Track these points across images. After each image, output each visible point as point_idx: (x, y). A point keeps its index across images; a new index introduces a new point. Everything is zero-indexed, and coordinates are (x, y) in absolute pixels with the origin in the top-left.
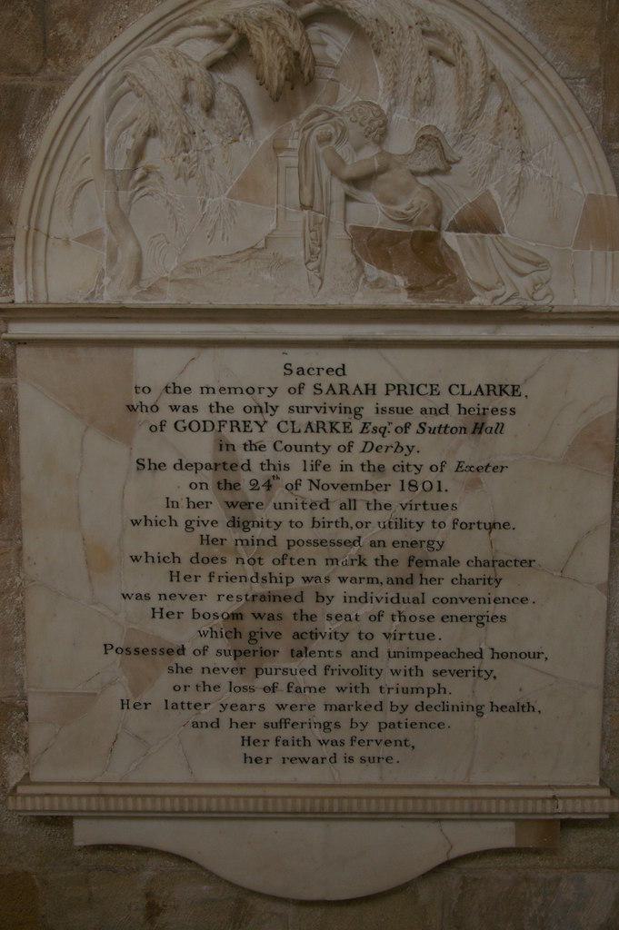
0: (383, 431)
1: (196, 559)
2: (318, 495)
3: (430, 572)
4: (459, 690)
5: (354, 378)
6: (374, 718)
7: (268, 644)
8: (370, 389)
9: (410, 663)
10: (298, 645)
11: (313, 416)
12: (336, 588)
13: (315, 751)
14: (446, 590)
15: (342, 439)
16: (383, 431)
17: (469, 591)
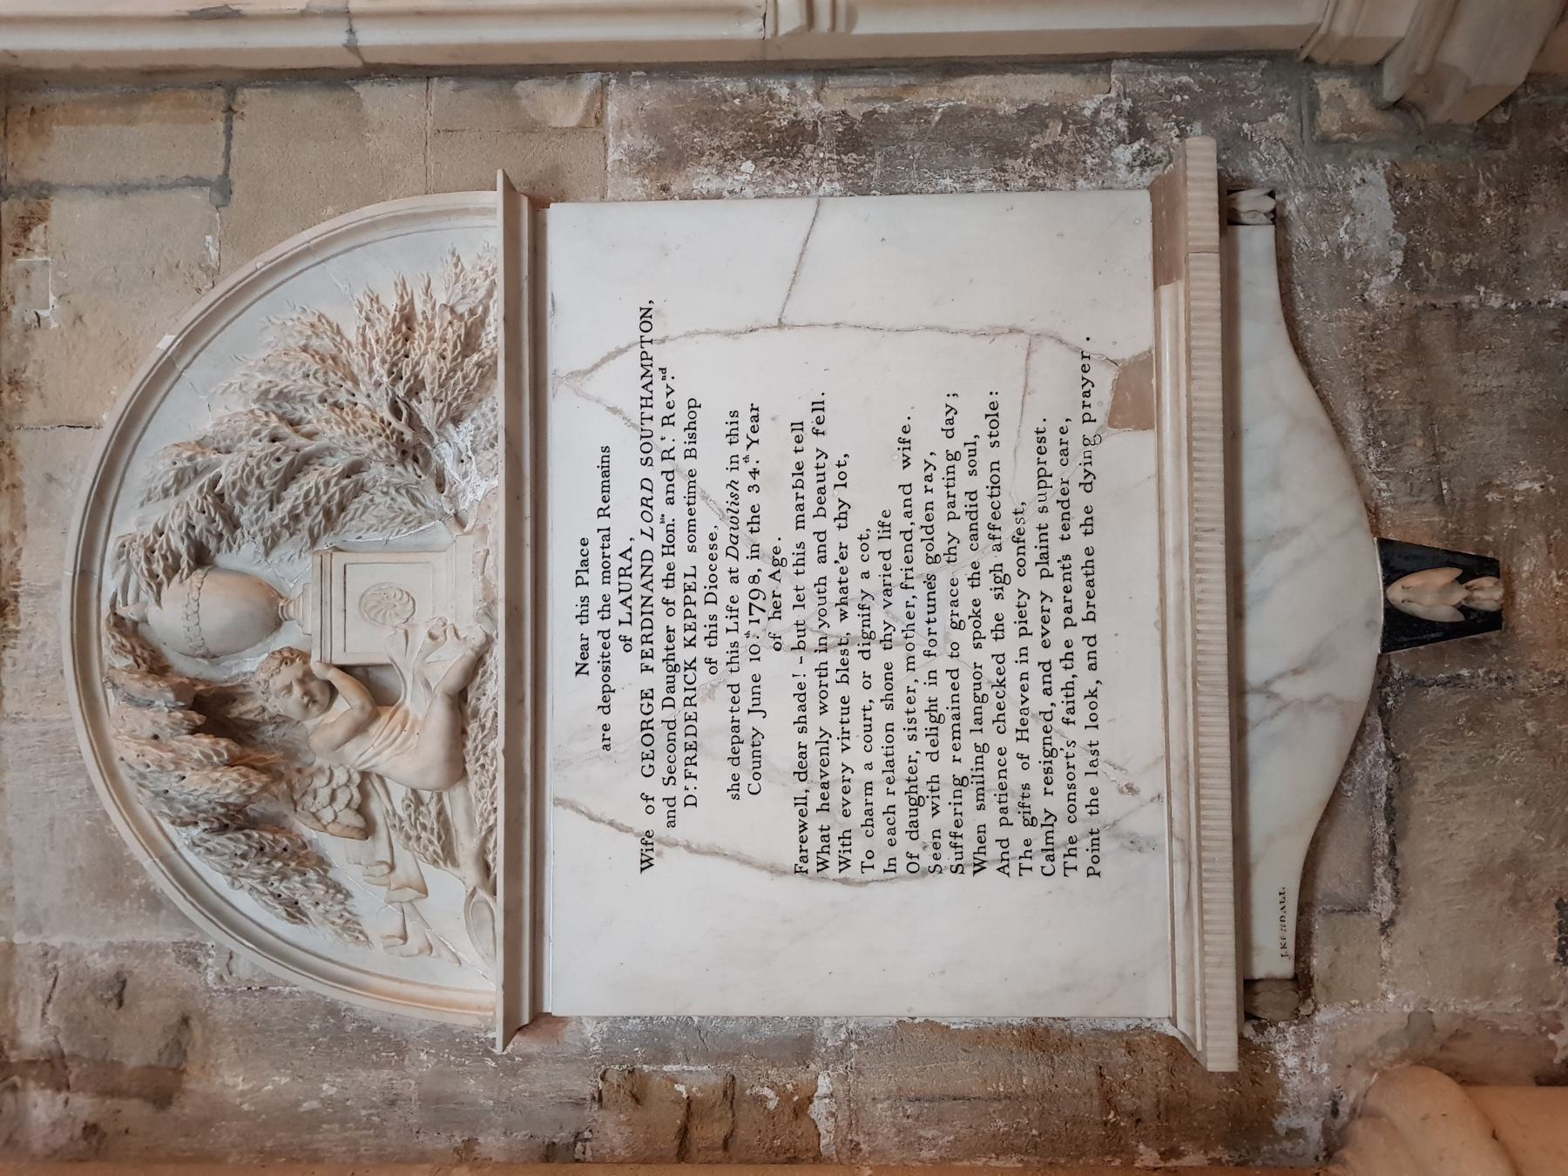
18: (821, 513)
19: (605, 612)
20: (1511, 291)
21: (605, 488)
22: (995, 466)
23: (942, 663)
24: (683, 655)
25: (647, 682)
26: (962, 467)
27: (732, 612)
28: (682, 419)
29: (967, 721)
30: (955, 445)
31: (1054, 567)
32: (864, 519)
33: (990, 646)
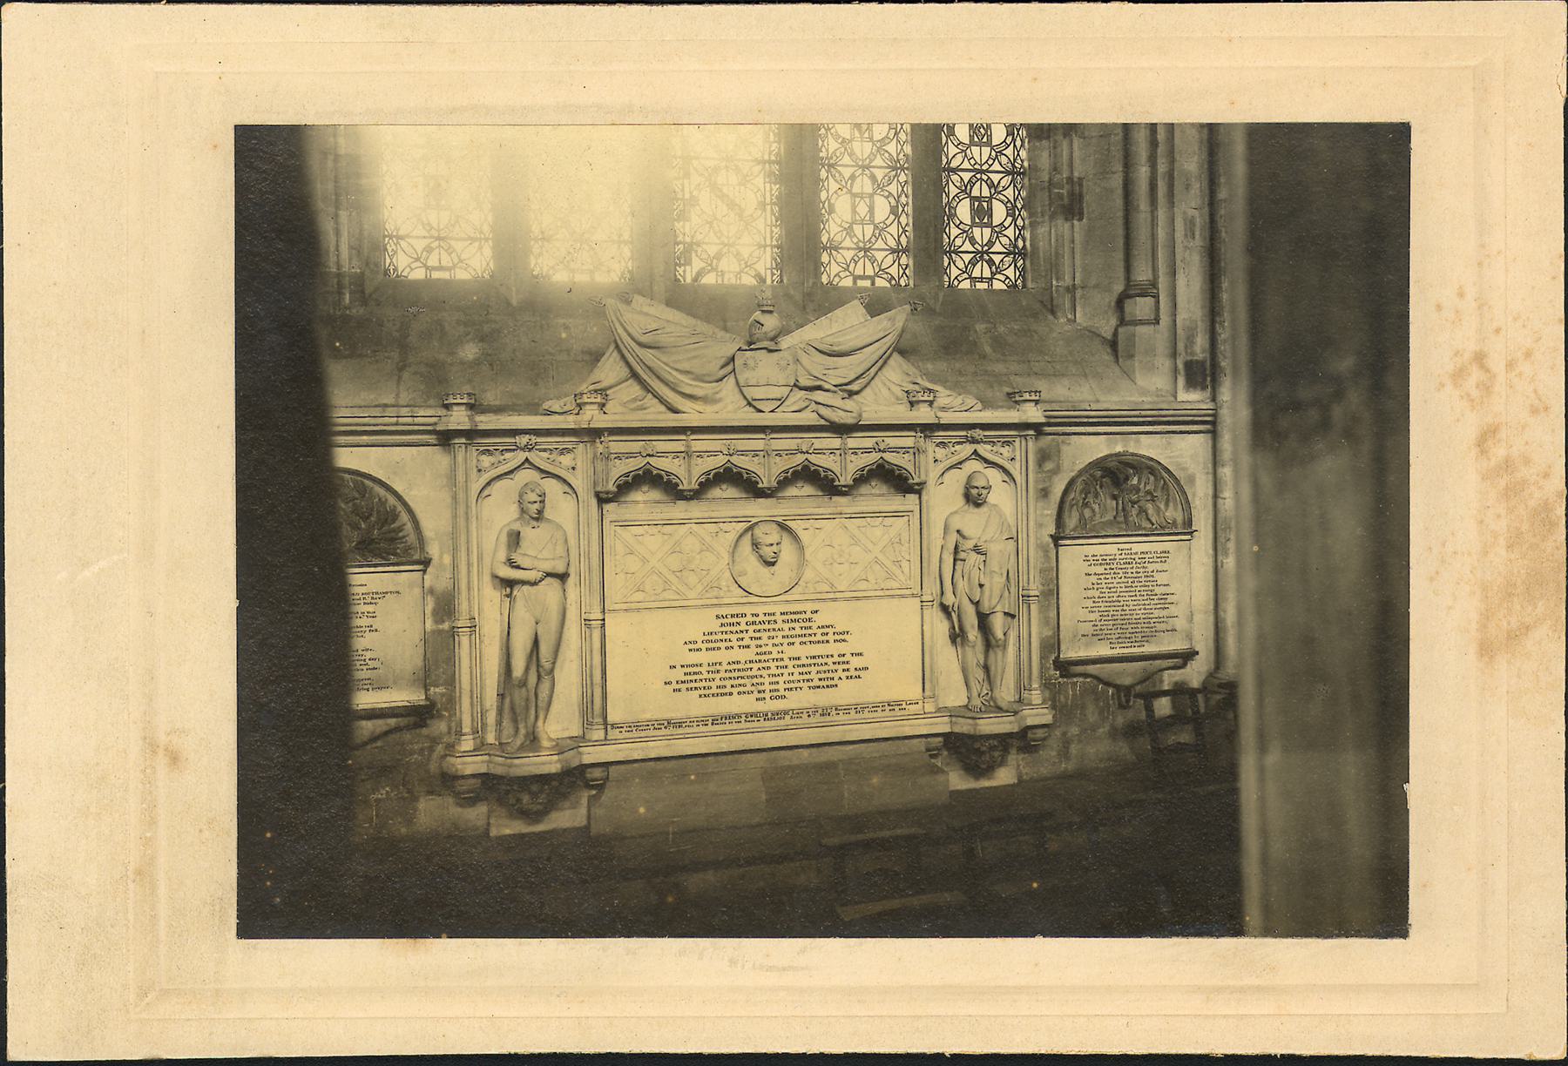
6: (1139, 635)
8: (1136, 553)
15: (1131, 566)
16: (1140, 564)
28: (373, 601)
30: (367, 661)
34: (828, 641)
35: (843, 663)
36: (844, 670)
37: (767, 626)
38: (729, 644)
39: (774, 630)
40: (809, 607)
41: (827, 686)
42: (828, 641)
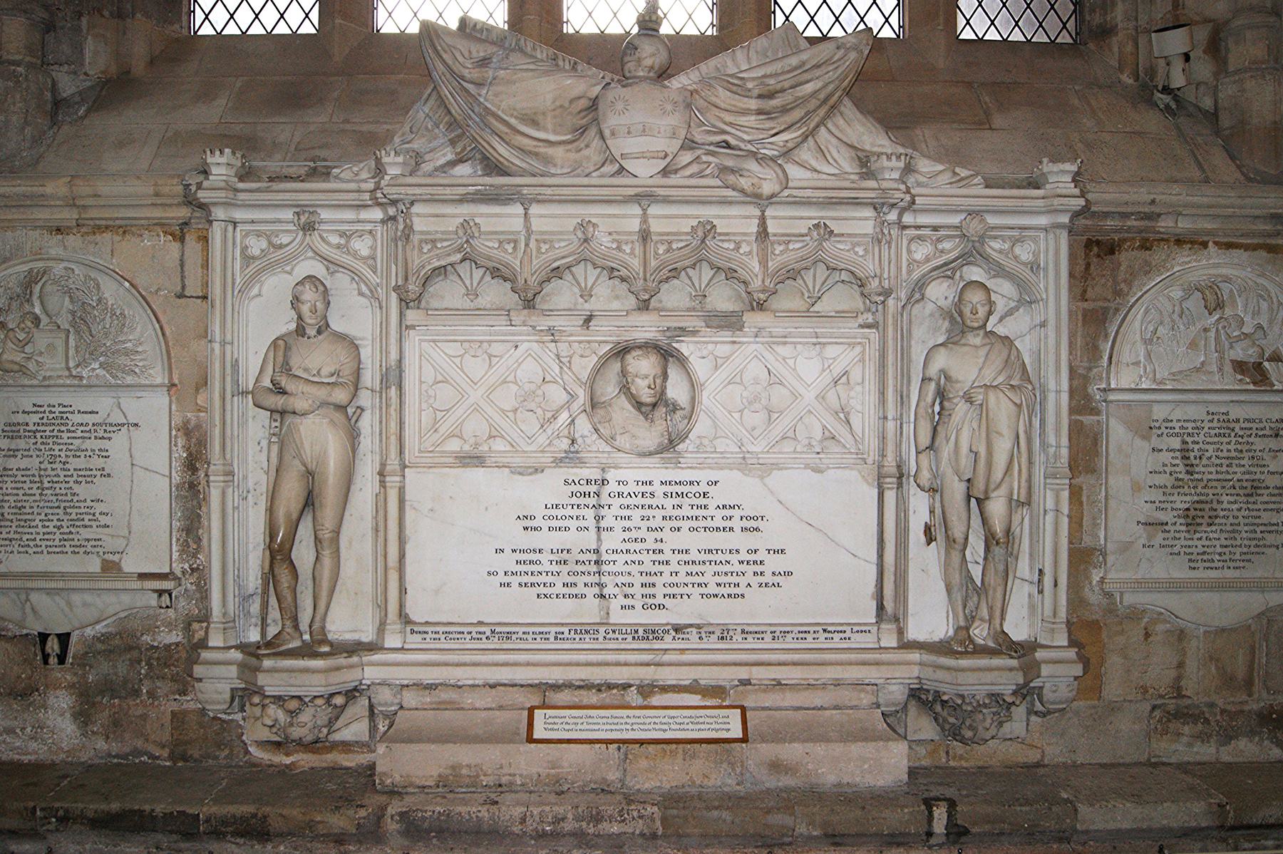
0: (1242, 437)
1: (1173, 487)
2: (1218, 462)
3: (1259, 491)
4: (1270, 539)
5: (1232, 416)
6: (1238, 550)
7: (1198, 520)
8: (1238, 421)
9: (1252, 528)
10: (1210, 521)
11: (1217, 431)
12: (1225, 498)
13: (1216, 564)
14: (1266, 498)
15: (1227, 440)
16: (1242, 437)
17: (1273, 499)
18: (78, 476)
19: (51, 412)
20: (146, 676)
21: (86, 413)
22: (91, 526)
23: (36, 510)
24: (38, 435)
25: (31, 424)
26: (91, 517)
27: (51, 449)
28: (106, 435)
29: (19, 517)
30: (97, 515)
31: (62, 543)
32: (77, 489)
33: (40, 524)
34: (731, 529)
35: (755, 562)
36: (755, 573)
37: (639, 501)
38: (583, 523)
39: (650, 507)
40: (703, 476)
41: (729, 596)
42: (731, 529)
